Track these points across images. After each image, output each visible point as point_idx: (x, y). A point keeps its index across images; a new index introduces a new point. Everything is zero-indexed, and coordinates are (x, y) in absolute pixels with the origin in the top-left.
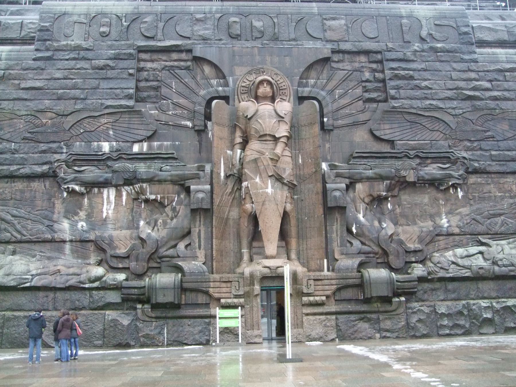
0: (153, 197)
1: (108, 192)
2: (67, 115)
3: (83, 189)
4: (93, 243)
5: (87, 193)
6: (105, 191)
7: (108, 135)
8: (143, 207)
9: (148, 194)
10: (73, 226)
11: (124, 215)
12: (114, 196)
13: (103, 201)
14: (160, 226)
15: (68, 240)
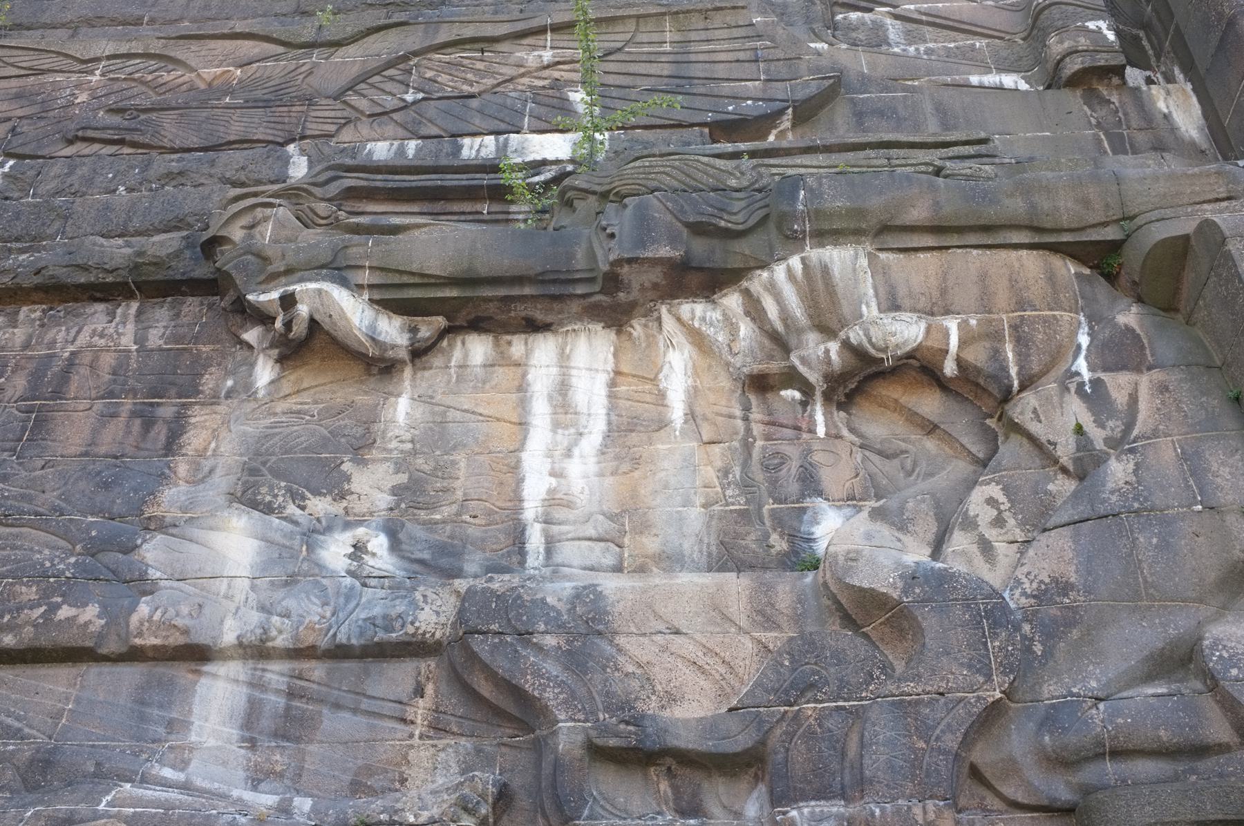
0: (907, 331)
1: (564, 359)
2: (338, 44)
3: (392, 331)
4: (428, 665)
5: (419, 353)
6: (542, 354)
7: (565, 108)
8: (821, 431)
9: (870, 310)
10: (291, 566)
11: (687, 484)
12: (602, 379)
13: (523, 404)
14: (999, 522)
15: (229, 638)
